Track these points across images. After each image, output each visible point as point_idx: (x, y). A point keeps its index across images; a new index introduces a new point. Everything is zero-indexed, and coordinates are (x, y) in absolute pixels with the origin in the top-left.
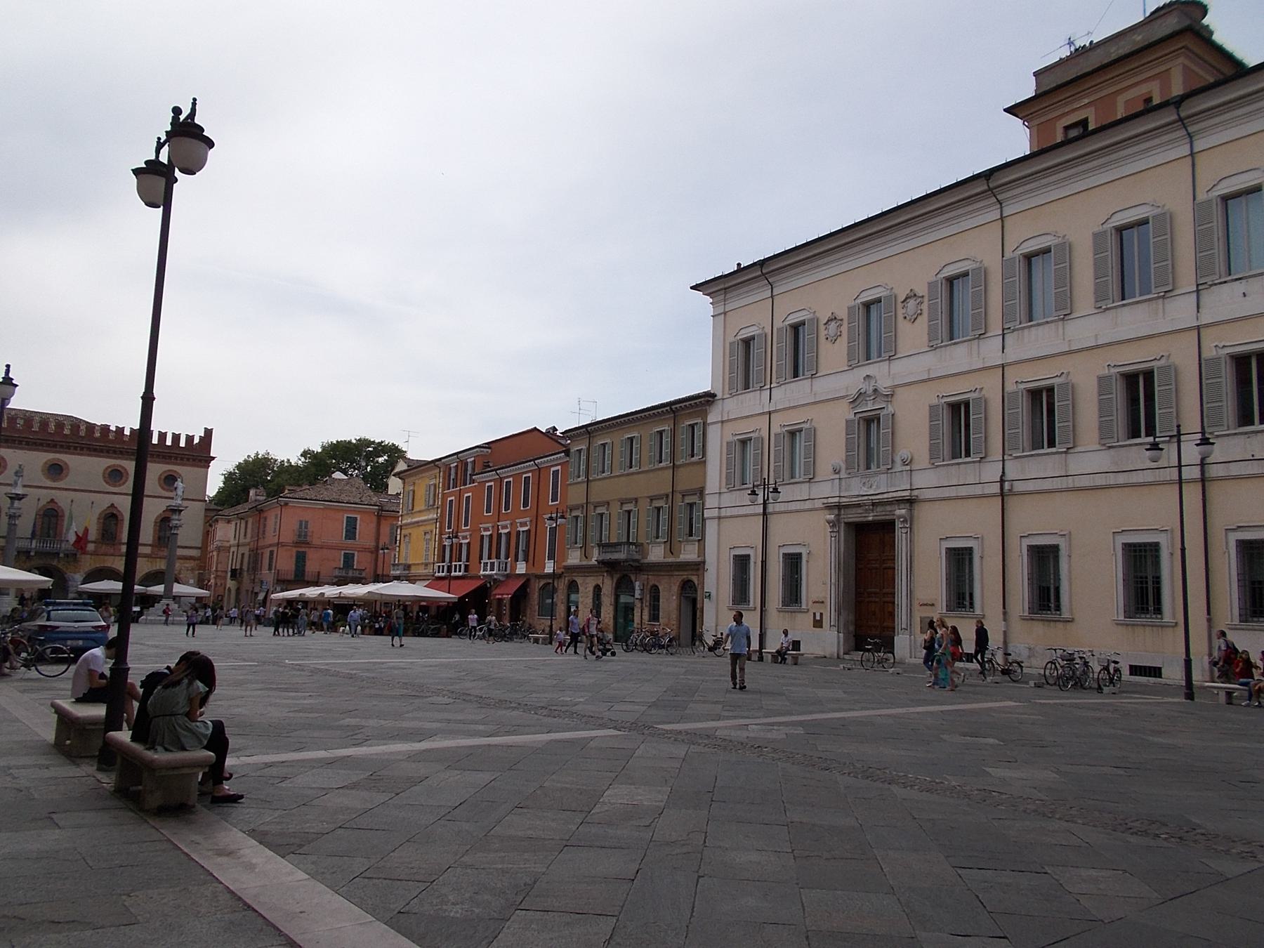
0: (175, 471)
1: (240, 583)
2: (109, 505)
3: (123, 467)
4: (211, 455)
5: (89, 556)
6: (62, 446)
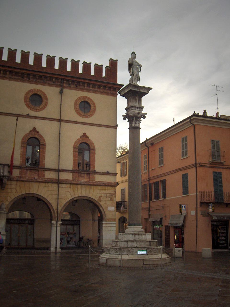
0: (89, 98)
2: (31, 129)
3: (43, 93)
5: (14, 183)
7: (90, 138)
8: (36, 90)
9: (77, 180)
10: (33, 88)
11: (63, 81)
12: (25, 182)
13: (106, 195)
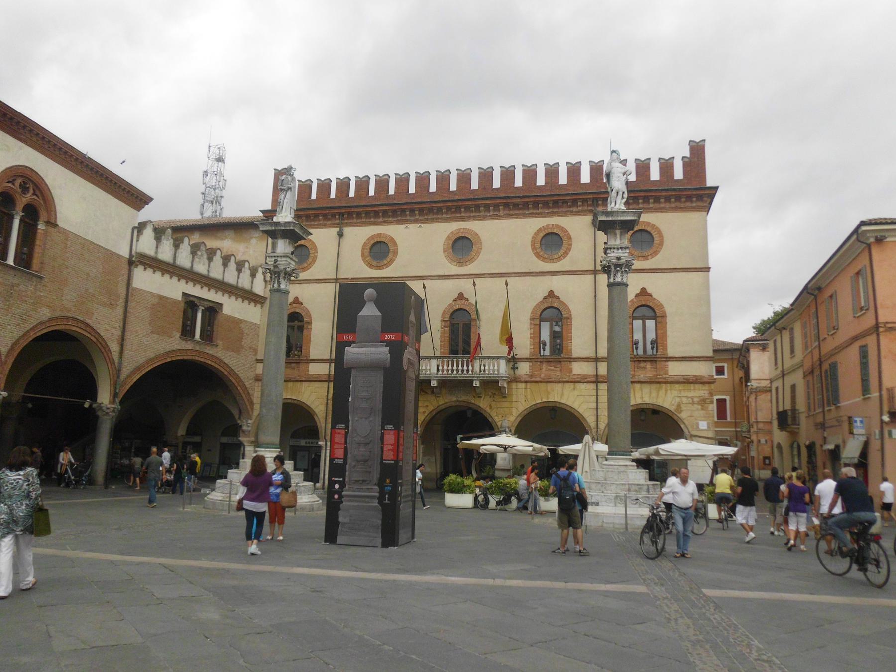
1: (794, 434)
2: (546, 294)
4: (710, 183)
5: (522, 385)
6: (468, 208)
7: (654, 296)
8: (551, 226)
9: (632, 375)
10: (544, 225)
11: (597, 201)
12: (540, 384)
13: (693, 401)
